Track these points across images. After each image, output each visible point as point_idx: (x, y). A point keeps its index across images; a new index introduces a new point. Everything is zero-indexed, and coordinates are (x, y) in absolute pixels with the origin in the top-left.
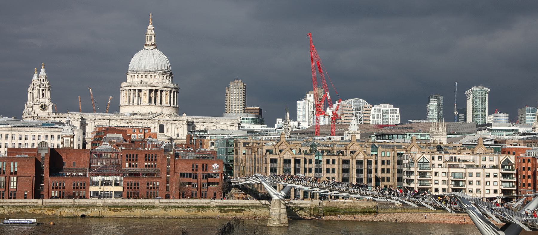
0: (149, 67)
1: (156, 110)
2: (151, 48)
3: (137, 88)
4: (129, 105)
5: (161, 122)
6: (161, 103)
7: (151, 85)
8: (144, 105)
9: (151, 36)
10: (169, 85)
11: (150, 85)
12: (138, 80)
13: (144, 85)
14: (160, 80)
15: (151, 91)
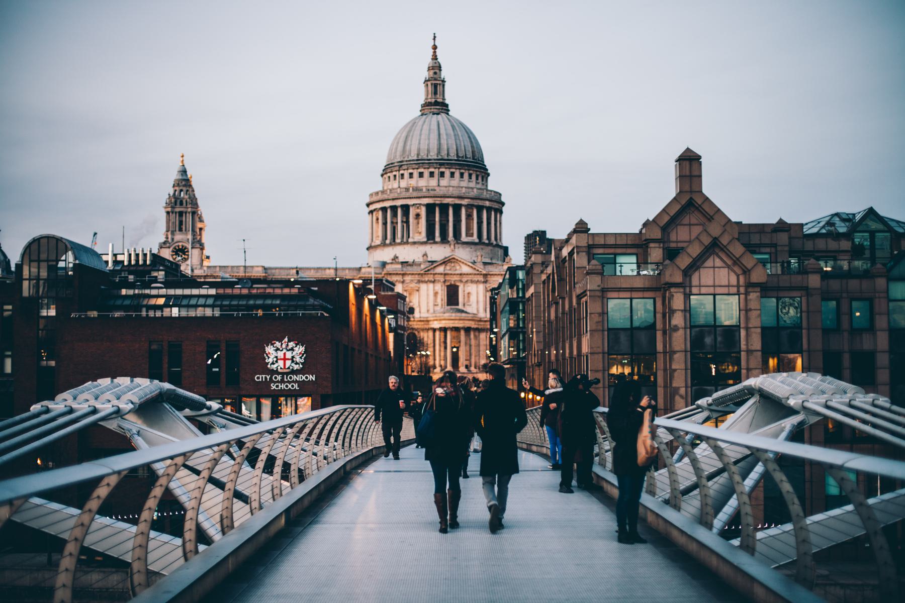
0: (428, 151)
1: (437, 252)
2: (436, 111)
3: (399, 203)
4: (384, 244)
5: (453, 279)
6: (457, 234)
7: (432, 193)
8: (414, 243)
9: (435, 86)
10: (475, 193)
11: (426, 194)
12: (404, 184)
13: (415, 194)
14: (456, 181)
15: (430, 208)
